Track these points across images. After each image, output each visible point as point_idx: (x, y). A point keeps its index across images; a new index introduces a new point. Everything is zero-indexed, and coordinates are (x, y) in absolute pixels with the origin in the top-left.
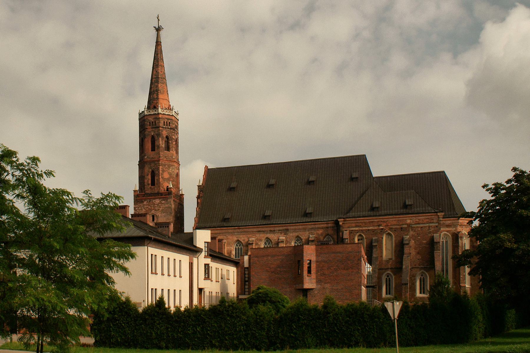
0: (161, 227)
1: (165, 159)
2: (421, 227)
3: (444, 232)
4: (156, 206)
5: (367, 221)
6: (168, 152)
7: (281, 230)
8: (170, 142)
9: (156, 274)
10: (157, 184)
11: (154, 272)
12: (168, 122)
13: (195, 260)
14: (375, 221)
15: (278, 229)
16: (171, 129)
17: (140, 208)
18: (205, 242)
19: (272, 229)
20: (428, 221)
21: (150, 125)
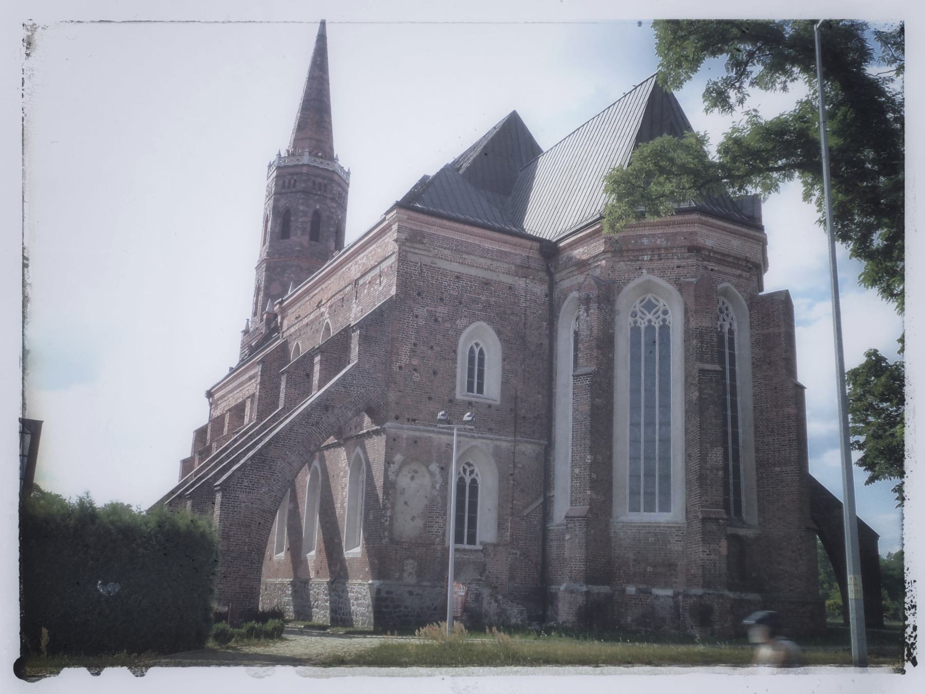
8: (292, 218)
12: (292, 182)
14: (316, 292)
16: (296, 192)
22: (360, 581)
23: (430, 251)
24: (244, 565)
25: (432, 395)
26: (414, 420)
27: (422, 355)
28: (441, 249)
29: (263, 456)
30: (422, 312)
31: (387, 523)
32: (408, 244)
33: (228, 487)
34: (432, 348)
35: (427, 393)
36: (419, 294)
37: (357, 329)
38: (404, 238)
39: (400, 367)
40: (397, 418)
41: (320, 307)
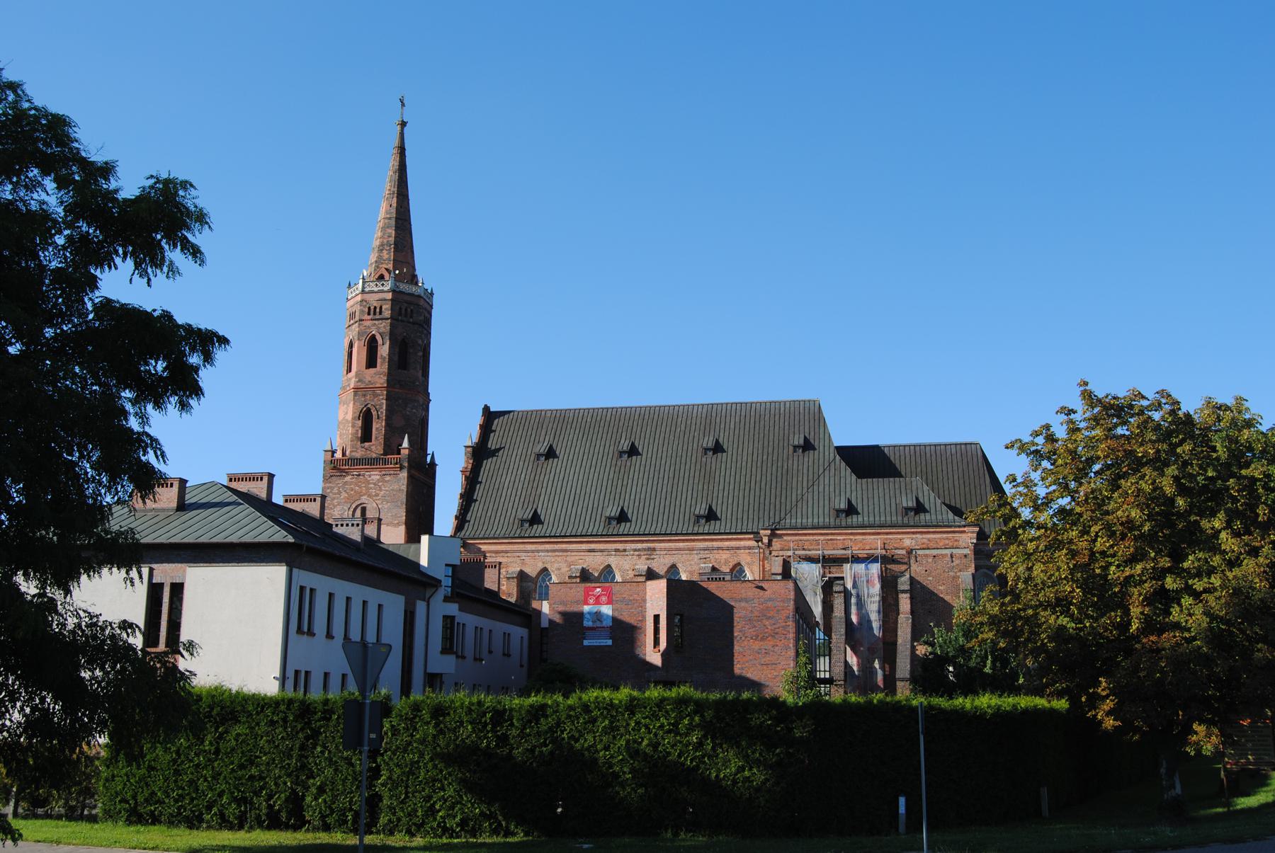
0: (353, 525)
2: (934, 556)
3: (981, 568)
4: (372, 486)
5: (822, 538)
6: (406, 372)
7: (639, 550)
8: (411, 351)
9: (311, 633)
10: (376, 438)
11: (306, 630)
13: (421, 607)
14: (838, 538)
15: (629, 546)
16: (414, 323)
17: (335, 490)
18: (447, 565)
19: (620, 548)
20: (948, 545)
21: (369, 314)
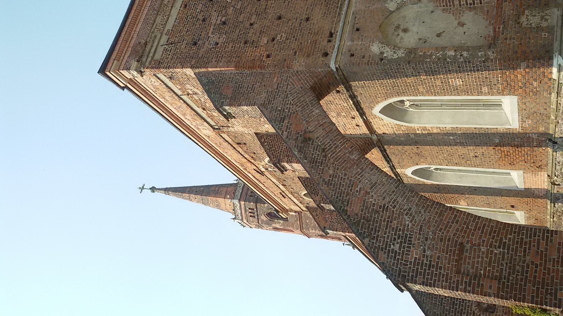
1: (298, 222)
12: (250, 211)
14: (251, 177)
22: (554, 95)
23: (156, 36)
24: (525, 255)
25: (304, 17)
26: (331, 35)
27: (258, 34)
28: (155, 25)
29: (359, 221)
30: (214, 38)
31: (465, 54)
32: (144, 59)
33: (399, 274)
34: (251, 24)
35: (301, 23)
36: (195, 44)
37: (225, 110)
38: (136, 63)
39: (268, 56)
40: (326, 54)
41: (262, 172)
